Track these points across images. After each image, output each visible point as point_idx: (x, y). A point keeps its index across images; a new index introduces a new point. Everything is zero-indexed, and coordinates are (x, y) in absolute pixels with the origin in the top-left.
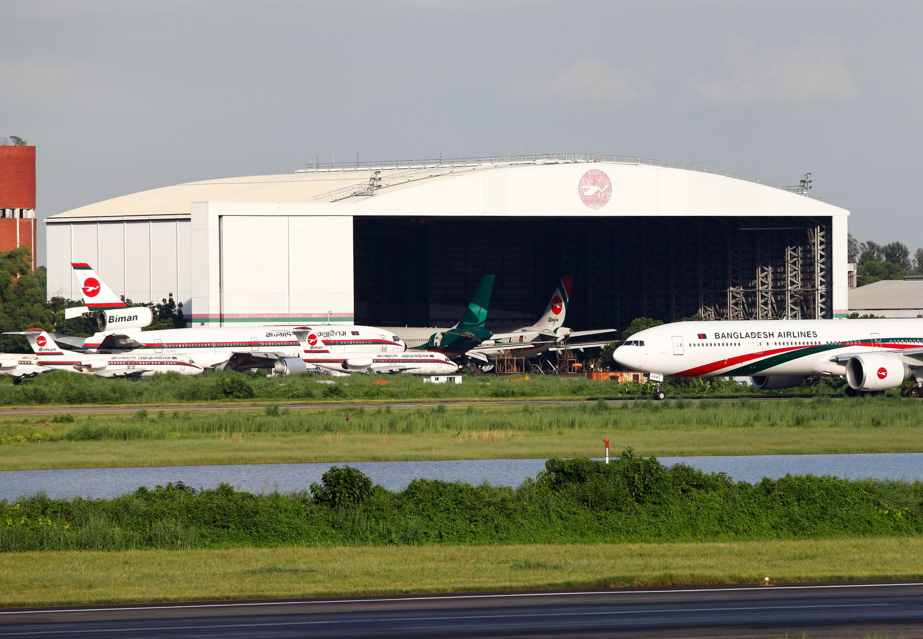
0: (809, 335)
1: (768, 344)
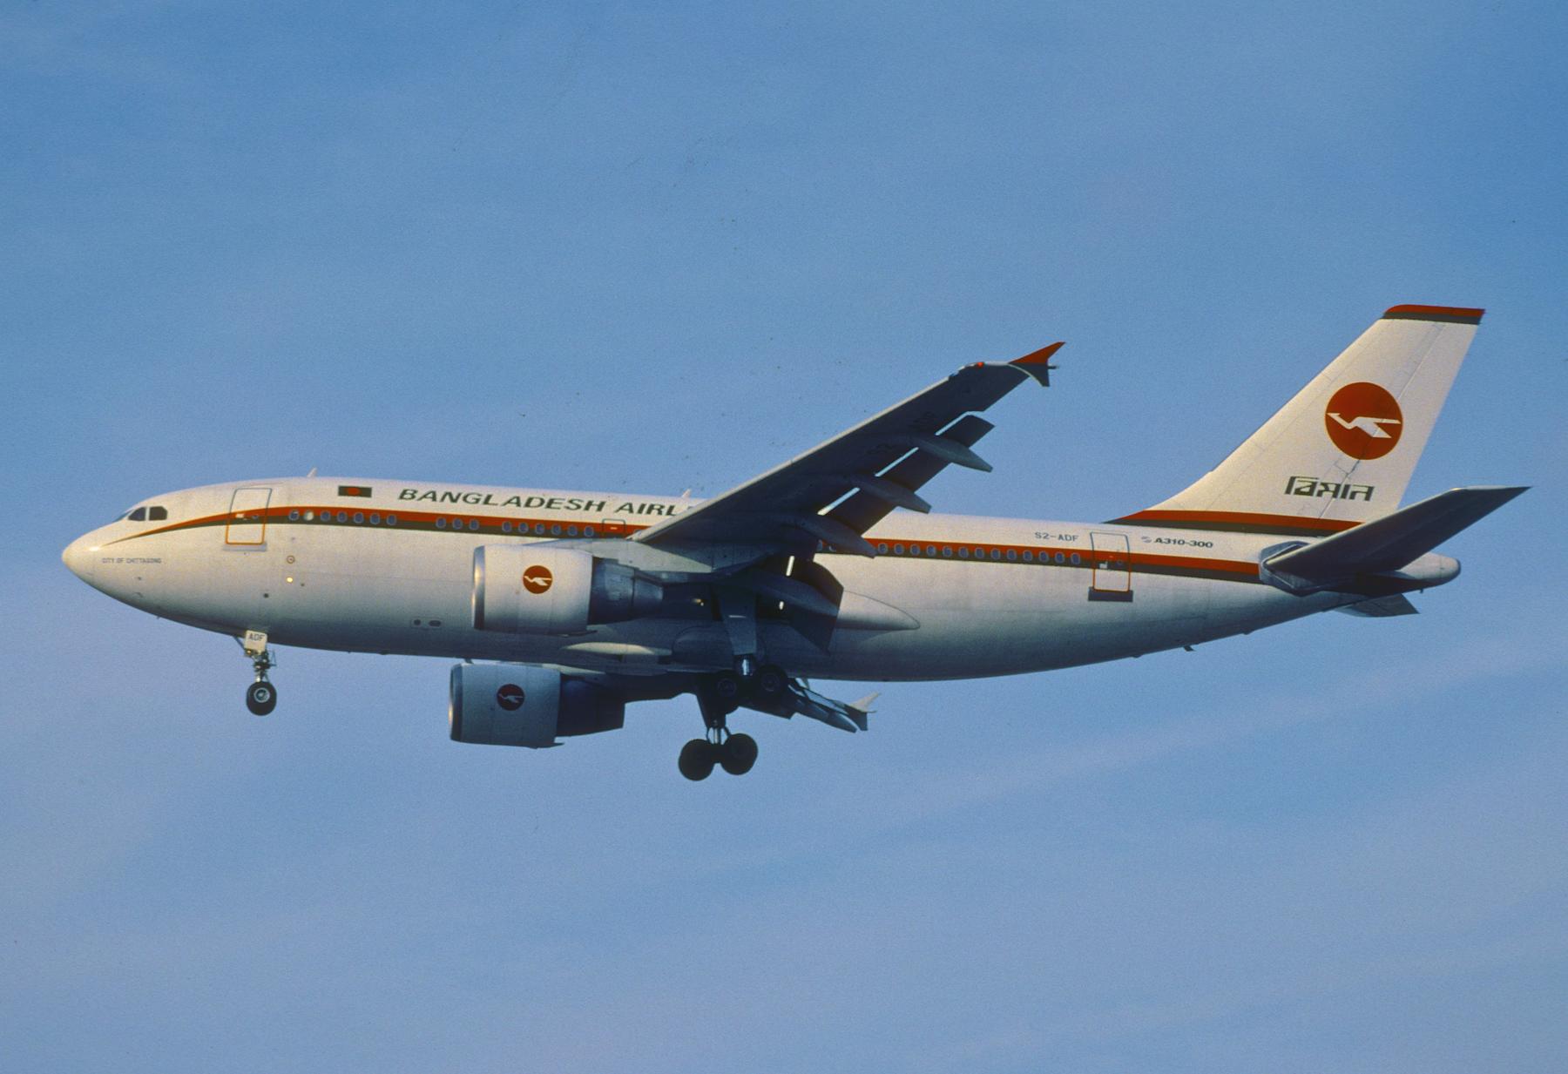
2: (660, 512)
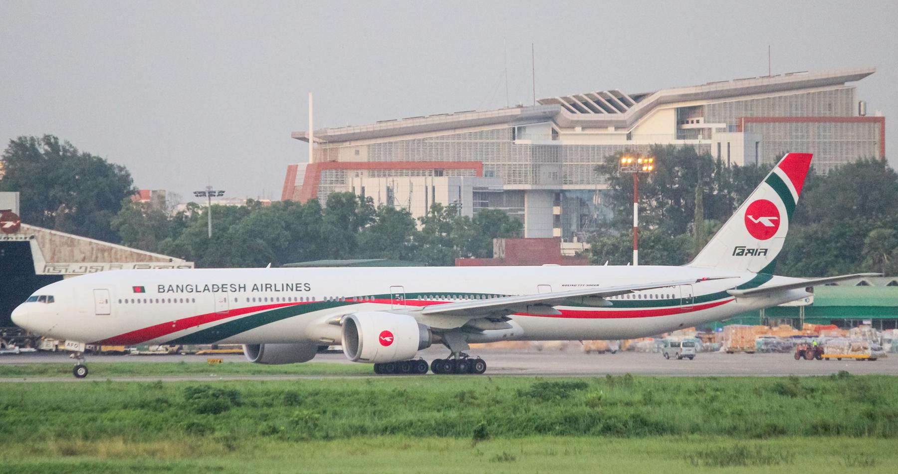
0: (298, 289)
1: (236, 300)
2: (271, 290)
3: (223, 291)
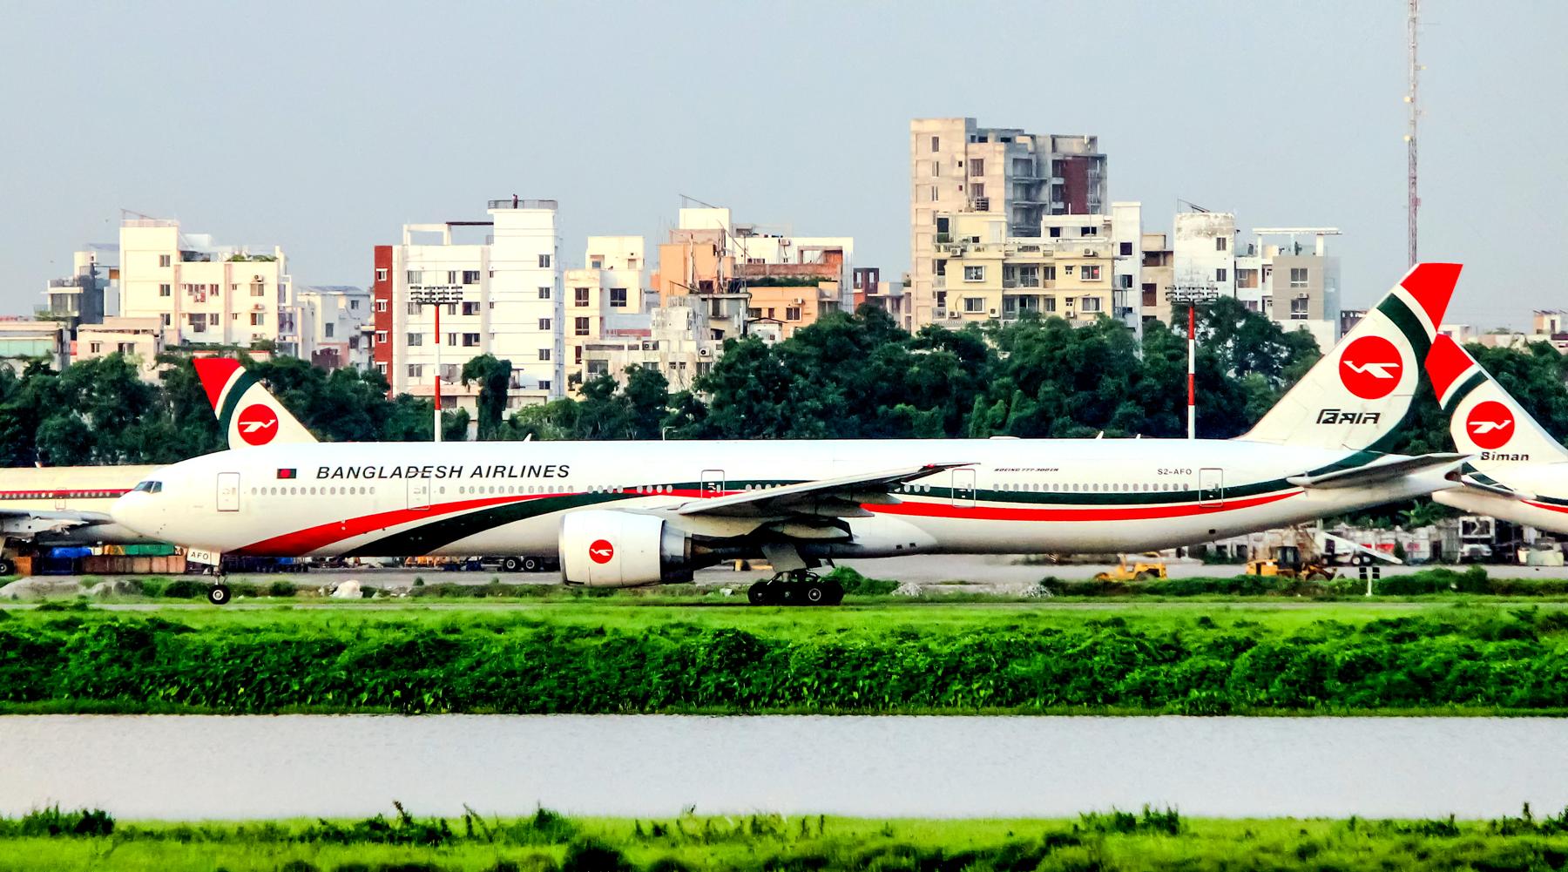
1: (442, 490)
3: (423, 476)
